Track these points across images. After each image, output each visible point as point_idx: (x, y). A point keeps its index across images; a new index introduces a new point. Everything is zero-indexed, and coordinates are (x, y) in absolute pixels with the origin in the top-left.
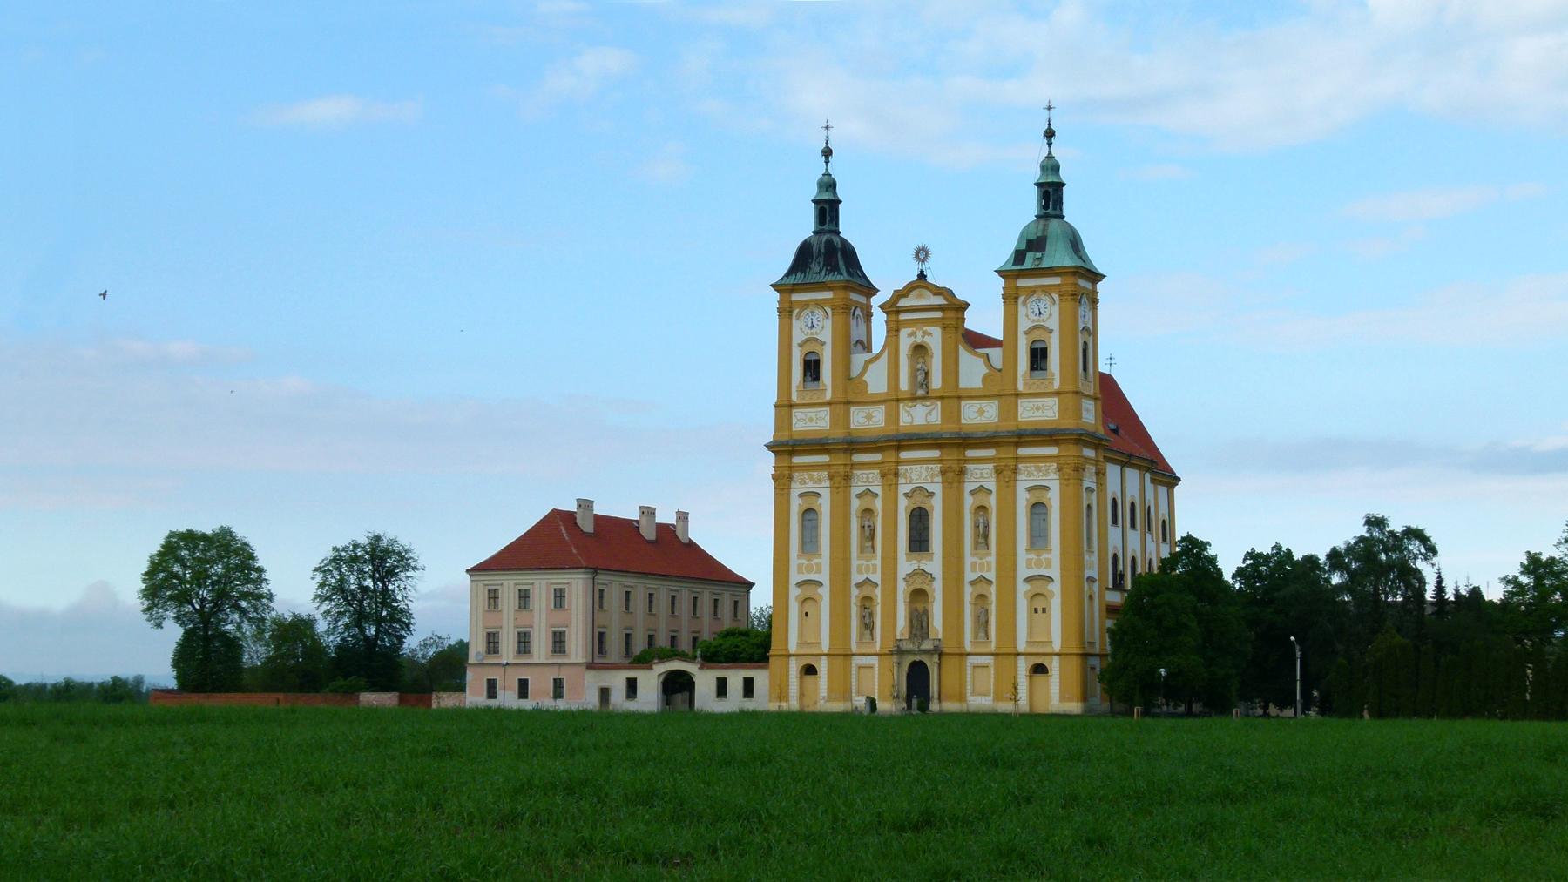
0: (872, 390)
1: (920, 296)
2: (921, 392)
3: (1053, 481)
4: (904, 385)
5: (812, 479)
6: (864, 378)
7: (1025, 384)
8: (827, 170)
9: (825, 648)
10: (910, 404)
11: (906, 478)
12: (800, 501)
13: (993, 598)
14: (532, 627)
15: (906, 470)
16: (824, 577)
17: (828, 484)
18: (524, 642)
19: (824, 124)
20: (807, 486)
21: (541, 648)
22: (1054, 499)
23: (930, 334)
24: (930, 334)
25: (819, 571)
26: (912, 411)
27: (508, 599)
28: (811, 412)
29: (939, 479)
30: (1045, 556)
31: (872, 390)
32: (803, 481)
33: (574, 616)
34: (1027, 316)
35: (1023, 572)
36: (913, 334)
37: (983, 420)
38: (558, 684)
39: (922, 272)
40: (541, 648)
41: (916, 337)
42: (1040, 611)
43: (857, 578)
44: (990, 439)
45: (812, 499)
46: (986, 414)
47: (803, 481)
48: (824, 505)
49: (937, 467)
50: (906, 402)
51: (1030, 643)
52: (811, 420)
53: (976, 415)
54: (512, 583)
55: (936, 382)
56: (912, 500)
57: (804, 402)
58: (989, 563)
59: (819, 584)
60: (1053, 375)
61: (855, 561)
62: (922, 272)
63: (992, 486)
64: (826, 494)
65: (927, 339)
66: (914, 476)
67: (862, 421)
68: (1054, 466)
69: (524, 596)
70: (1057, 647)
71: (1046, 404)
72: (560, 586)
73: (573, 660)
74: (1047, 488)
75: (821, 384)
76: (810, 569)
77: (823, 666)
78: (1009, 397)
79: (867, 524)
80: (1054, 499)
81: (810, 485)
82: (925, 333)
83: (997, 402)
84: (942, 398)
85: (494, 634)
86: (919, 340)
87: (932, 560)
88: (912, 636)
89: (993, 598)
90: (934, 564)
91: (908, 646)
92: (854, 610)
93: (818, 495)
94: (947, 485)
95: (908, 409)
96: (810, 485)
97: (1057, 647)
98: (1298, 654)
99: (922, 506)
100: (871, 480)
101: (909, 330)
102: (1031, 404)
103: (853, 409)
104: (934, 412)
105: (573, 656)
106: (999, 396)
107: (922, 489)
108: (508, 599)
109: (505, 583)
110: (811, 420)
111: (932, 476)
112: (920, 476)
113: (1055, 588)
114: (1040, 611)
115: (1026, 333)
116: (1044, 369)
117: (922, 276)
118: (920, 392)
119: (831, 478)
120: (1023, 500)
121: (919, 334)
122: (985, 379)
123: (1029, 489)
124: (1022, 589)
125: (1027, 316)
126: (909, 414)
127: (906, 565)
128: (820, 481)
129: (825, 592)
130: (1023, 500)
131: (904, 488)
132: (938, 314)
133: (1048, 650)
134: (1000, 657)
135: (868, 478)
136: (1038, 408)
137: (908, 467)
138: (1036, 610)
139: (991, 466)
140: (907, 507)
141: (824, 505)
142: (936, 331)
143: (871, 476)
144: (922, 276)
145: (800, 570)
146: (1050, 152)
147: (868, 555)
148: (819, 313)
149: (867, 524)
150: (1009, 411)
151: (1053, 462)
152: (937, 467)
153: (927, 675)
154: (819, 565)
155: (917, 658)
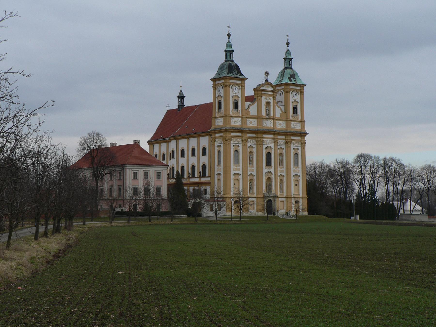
1: (268, 87)
2: (268, 117)
4: (264, 114)
7: (292, 118)
8: (229, 41)
10: (266, 120)
11: (265, 143)
15: (265, 140)
16: (240, 172)
17: (241, 143)
19: (228, 26)
20: (235, 143)
23: (271, 99)
24: (271, 99)
25: (239, 170)
26: (266, 122)
28: (236, 119)
29: (273, 144)
30: (298, 169)
32: (234, 141)
33: (140, 182)
34: (292, 97)
35: (293, 174)
36: (267, 99)
37: (236, 124)
39: (267, 79)
41: (267, 99)
42: (296, 185)
43: (293, 174)
46: (282, 125)
47: (234, 141)
48: (240, 149)
49: (273, 140)
50: (264, 119)
52: (236, 122)
53: (279, 125)
54: (142, 170)
55: (272, 115)
56: (267, 150)
57: (233, 115)
58: (283, 170)
59: (239, 175)
60: (299, 116)
61: (216, 167)
62: (267, 79)
63: (284, 147)
64: (241, 145)
65: (270, 101)
66: (267, 143)
67: (249, 123)
68: (300, 143)
70: (301, 196)
71: (298, 124)
72: (147, 172)
74: (298, 149)
75: (238, 111)
76: (236, 170)
78: (287, 121)
79: (251, 156)
81: (236, 142)
82: (270, 99)
83: (285, 122)
84: (257, 118)
86: (268, 101)
87: (272, 169)
88: (268, 192)
89: (285, 181)
91: (267, 195)
92: (249, 183)
93: (239, 146)
94: (275, 147)
95: (265, 122)
96: (236, 142)
99: (270, 152)
100: (252, 143)
101: (265, 97)
102: (294, 124)
104: (272, 123)
107: (270, 147)
109: (140, 170)
110: (236, 122)
111: (272, 143)
112: (269, 142)
113: (300, 178)
114: (296, 185)
115: (292, 102)
116: (221, 109)
117: (267, 80)
118: (268, 117)
119: (242, 141)
120: (292, 152)
121: (268, 99)
122: (281, 115)
125: (292, 97)
126: (266, 123)
127: (265, 170)
128: (239, 142)
129: (241, 177)
130: (292, 152)
132: (272, 93)
134: (259, 198)
135: (251, 142)
136: (296, 125)
137: (266, 140)
138: (295, 185)
140: (265, 152)
141: (240, 149)
142: (272, 98)
143: (251, 141)
144: (267, 80)
145: (234, 171)
146: (288, 49)
147: (251, 166)
149: (251, 156)
151: (300, 141)
152: (273, 140)
154: (299, 170)
155: (270, 199)
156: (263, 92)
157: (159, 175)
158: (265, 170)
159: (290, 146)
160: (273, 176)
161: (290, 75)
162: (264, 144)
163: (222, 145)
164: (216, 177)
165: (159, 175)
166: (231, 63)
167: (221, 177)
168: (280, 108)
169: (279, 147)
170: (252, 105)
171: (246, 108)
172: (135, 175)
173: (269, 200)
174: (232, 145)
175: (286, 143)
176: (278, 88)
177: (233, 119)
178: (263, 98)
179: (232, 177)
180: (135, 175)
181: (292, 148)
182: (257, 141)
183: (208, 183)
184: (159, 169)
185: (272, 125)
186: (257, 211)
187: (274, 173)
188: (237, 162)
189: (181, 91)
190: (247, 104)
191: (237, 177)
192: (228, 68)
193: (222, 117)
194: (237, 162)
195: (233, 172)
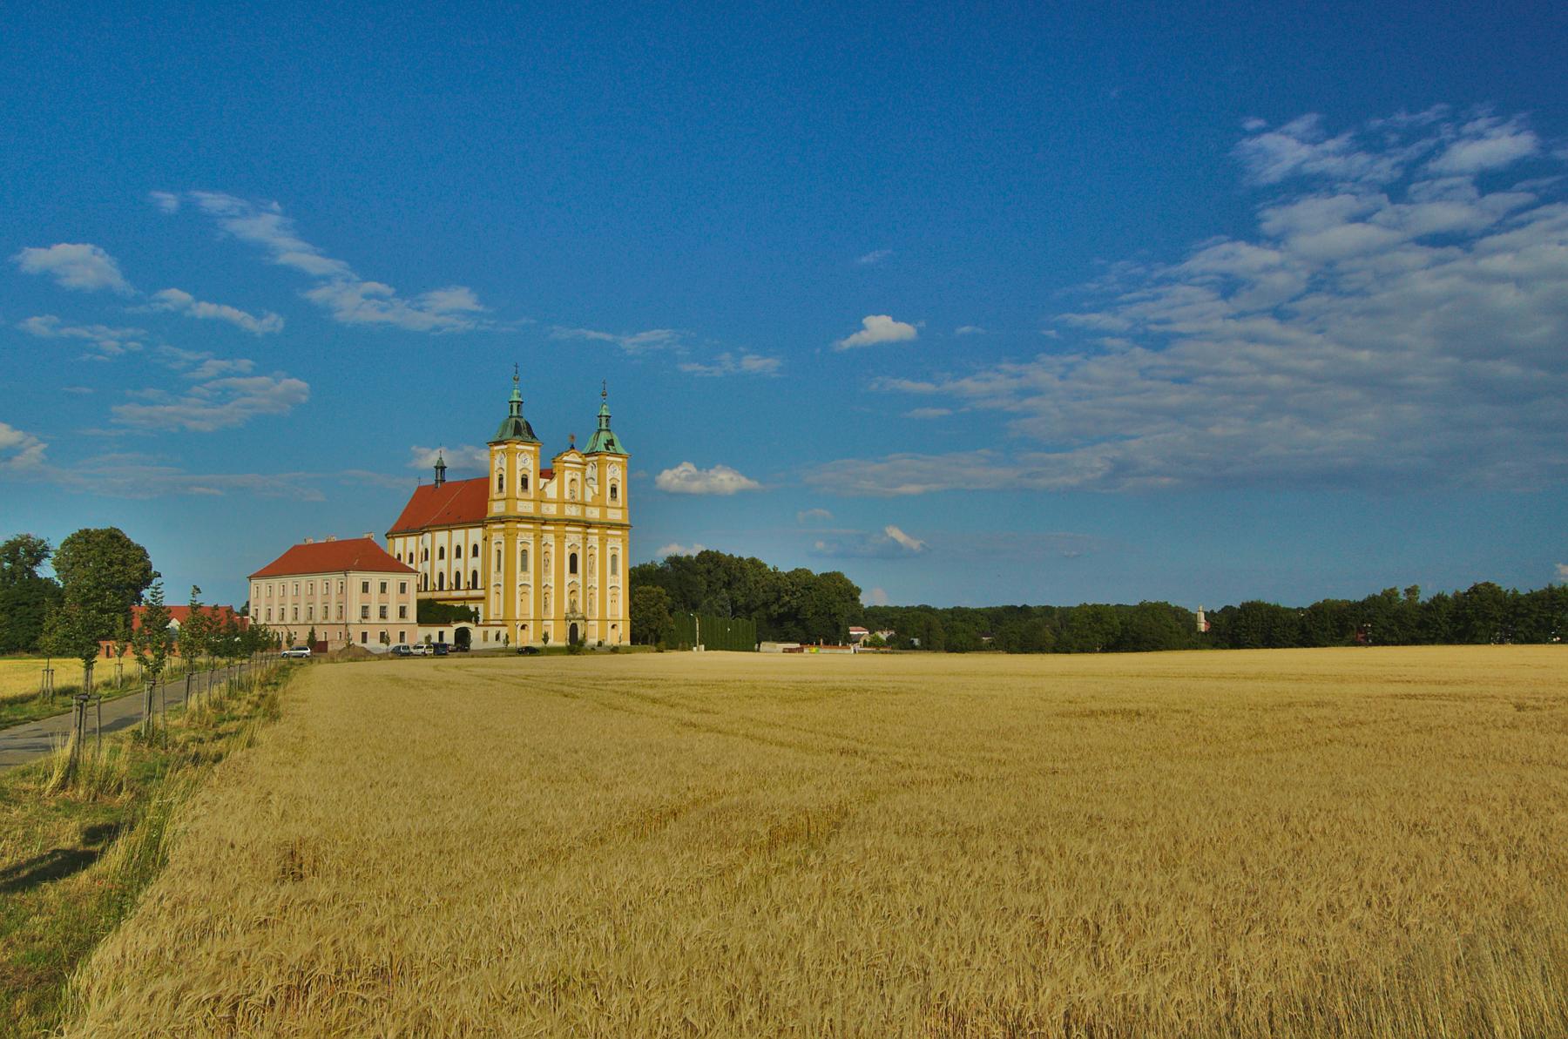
0: (548, 496)
3: (620, 546)
4: (567, 496)
5: (525, 535)
6: (546, 490)
9: (532, 617)
12: (569, 550)
13: (597, 595)
14: (370, 603)
16: (531, 583)
18: (383, 613)
21: (393, 614)
22: (620, 553)
27: (374, 588)
29: (581, 541)
31: (548, 496)
32: (522, 537)
35: (609, 585)
36: (570, 474)
37: (525, 510)
38: (402, 634)
40: (393, 614)
43: (609, 585)
44: (556, 521)
45: (526, 545)
47: (522, 537)
49: (581, 536)
51: (611, 615)
64: (532, 543)
69: (383, 586)
73: (411, 622)
74: (618, 549)
77: (531, 625)
78: (604, 507)
80: (620, 553)
85: (367, 607)
90: (579, 579)
91: (571, 616)
93: (529, 544)
97: (621, 617)
98: (697, 620)
101: (569, 472)
103: (543, 504)
105: (372, 618)
106: (600, 506)
108: (374, 588)
113: (620, 591)
120: (609, 553)
123: (611, 548)
124: (609, 591)
129: (532, 590)
130: (609, 553)
131: (567, 544)
132: (579, 466)
133: (616, 618)
139: (597, 537)
142: (579, 473)
148: (528, 456)
150: (604, 514)
153: (577, 629)
155: (574, 622)
156: (566, 465)
157: (403, 587)
158: (568, 578)
159: (605, 545)
160: (581, 589)
161: (608, 441)
162: (566, 540)
163: (503, 542)
164: (493, 590)
165: (403, 587)
166: (519, 420)
167: (501, 589)
168: (592, 488)
169: (589, 545)
170: (549, 483)
171: (541, 487)
172: (365, 587)
173: (573, 624)
174: (518, 542)
175: (600, 540)
176: (588, 459)
177: (520, 503)
178: (567, 473)
179: (518, 589)
180: (365, 587)
181: (609, 547)
182: (556, 537)
183: (482, 598)
184: (403, 577)
185: (579, 513)
186: (555, 640)
187: (581, 583)
188: (524, 568)
189: (441, 458)
190: (543, 481)
191: (525, 588)
192: (514, 426)
193: (504, 499)
194: (524, 568)
195: (518, 583)
